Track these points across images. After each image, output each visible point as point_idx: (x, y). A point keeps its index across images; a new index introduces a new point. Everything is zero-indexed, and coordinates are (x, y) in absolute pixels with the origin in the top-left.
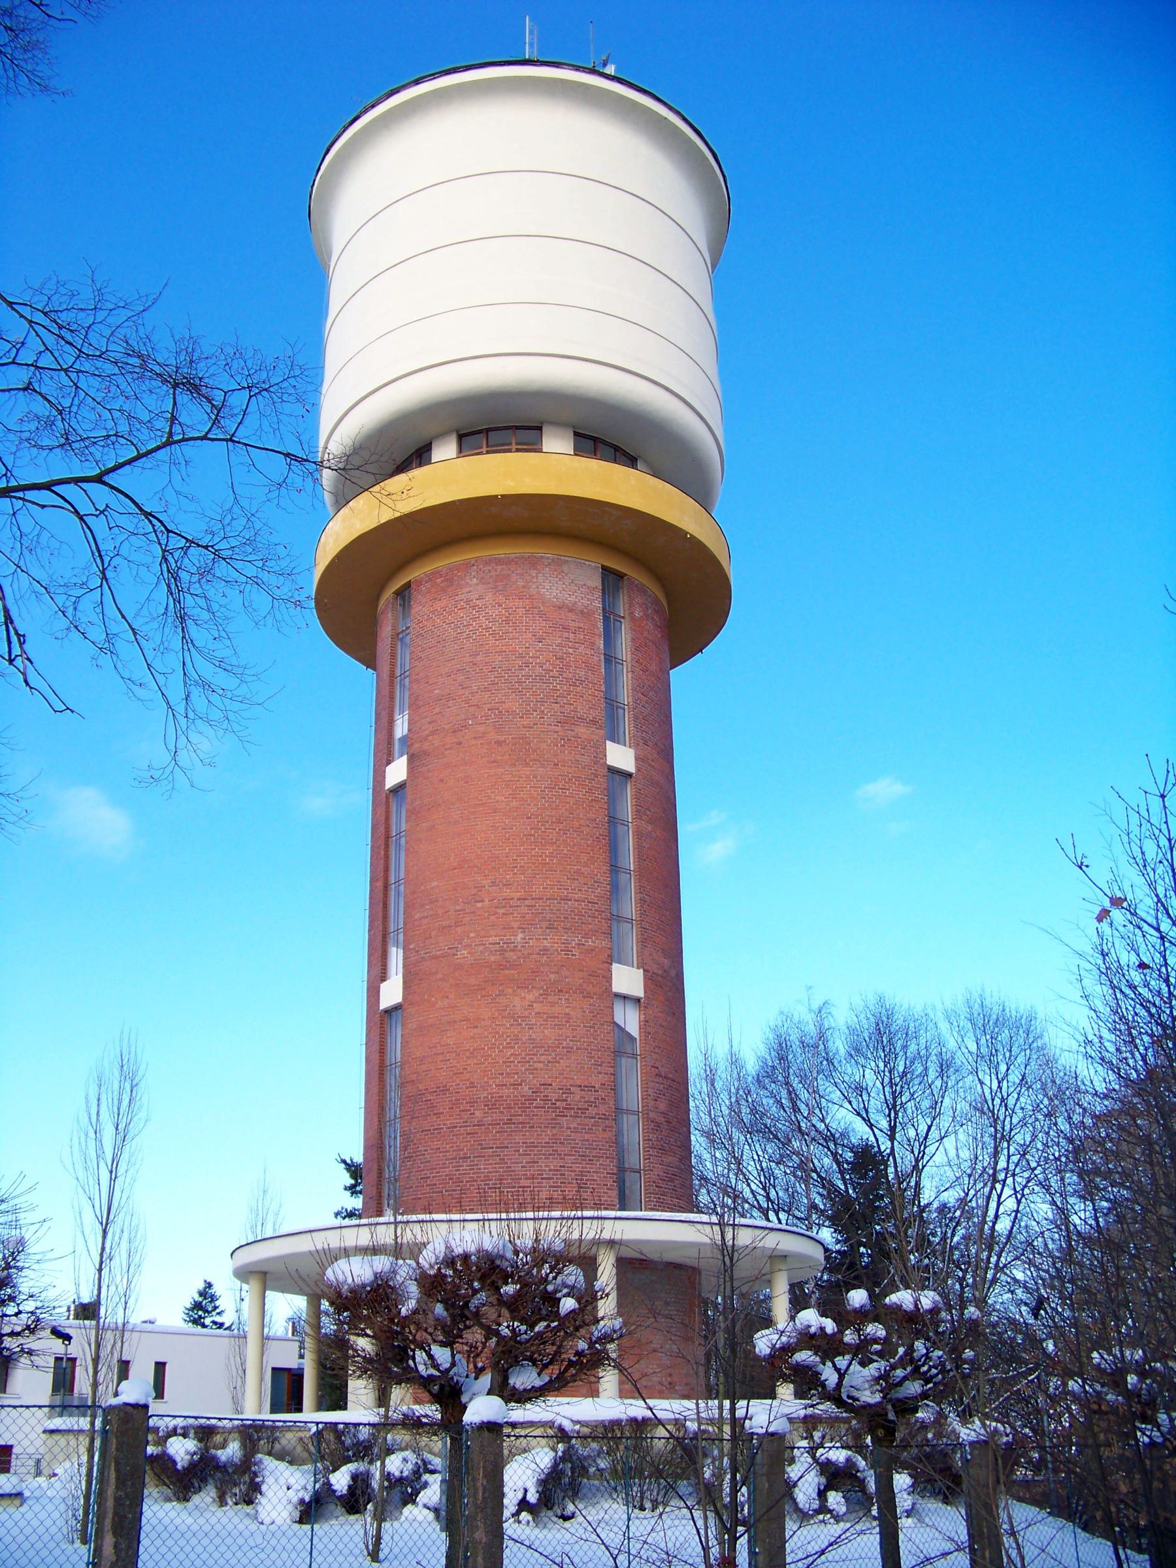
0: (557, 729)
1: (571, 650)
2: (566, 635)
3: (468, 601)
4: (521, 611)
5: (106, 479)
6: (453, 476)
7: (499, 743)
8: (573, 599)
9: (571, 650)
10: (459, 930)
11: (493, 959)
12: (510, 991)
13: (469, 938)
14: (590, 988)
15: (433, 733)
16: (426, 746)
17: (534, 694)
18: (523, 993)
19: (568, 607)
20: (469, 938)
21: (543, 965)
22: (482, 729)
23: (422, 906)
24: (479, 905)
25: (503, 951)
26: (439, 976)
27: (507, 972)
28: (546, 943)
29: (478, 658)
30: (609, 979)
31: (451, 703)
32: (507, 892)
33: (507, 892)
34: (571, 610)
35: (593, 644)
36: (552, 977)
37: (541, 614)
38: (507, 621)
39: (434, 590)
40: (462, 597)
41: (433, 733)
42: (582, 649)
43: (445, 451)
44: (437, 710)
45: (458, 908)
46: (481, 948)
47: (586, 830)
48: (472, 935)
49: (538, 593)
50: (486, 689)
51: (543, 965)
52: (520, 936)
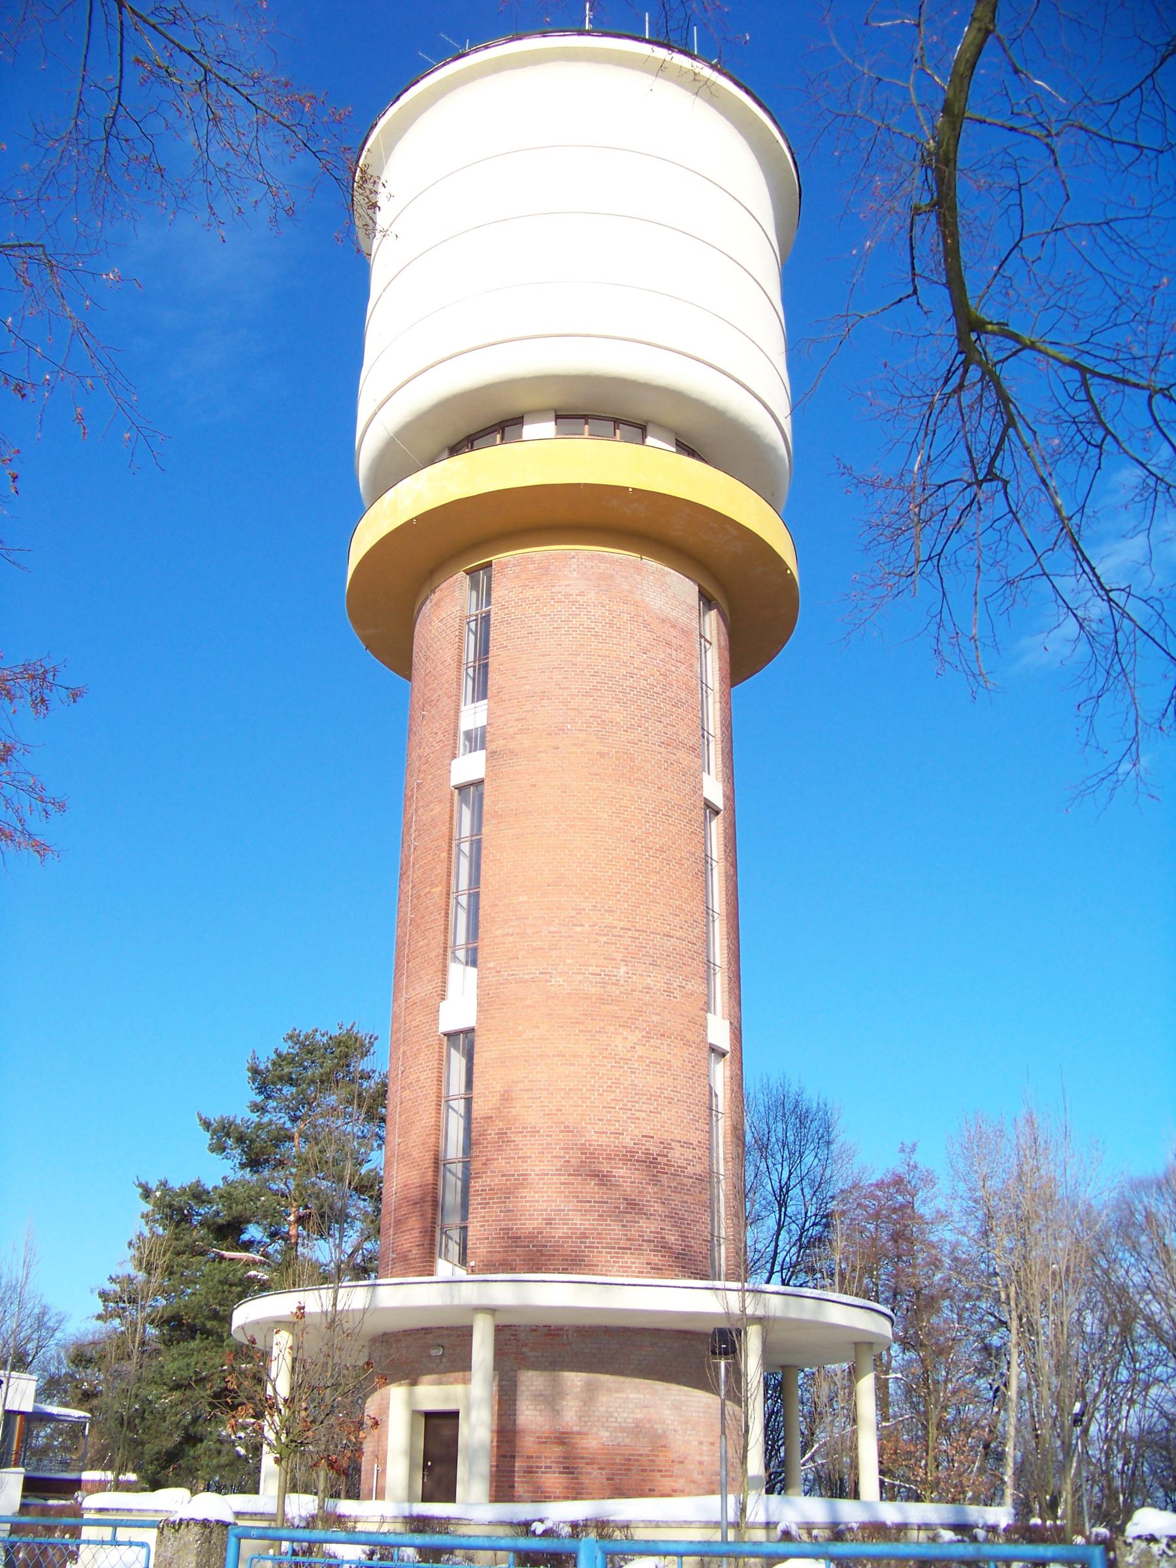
0: (662, 750)
1: (673, 669)
2: (669, 651)
3: (567, 595)
4: (626, 617)
5: (1109, 438)
6: (541, 458)
7: (602, 755)
8: (674, 613)
9: (673, 669)
10: (554, 954)
11: (593, 990)
12: (612, 1029)
13: (565, 964)
14: (689, 1036)
15: (521, 732)
16: (512, 745)
17: (639, 708)
18: (626, 1032)
19: (670, 622)
20: (565, 964)
21: (646, 1004)
22: (583, 736)
23: (506, 922)
24: (579, 929)
25: (604, 984)
26: (529, 1002)
27: (608, 1007)
28: (649, 980)
29: (579, 659)
30: (705, 1027)
31: (545, 702)
32: (609, 919)
33: (609, 919)
34: (674, 626)
35: (691, 665)
36: (655, 1018)
37: (646, 625)
38: (611, 625)
39: (524, 576)
40: (560, 589)
41: (521, 732)
42: (682, 668)
43: (539, 430)
44: (528, 707)
45: (552, 929)
46: (580, 977)
47: (687, 864)
48: (569, 961)
49: (643, 601)
50: (587, 694)
51: (646, 1004)
52: (623, 969)
